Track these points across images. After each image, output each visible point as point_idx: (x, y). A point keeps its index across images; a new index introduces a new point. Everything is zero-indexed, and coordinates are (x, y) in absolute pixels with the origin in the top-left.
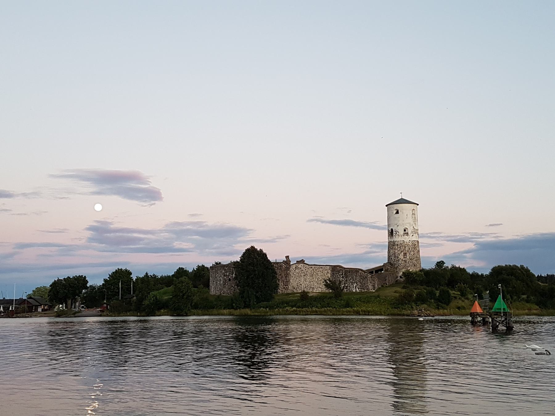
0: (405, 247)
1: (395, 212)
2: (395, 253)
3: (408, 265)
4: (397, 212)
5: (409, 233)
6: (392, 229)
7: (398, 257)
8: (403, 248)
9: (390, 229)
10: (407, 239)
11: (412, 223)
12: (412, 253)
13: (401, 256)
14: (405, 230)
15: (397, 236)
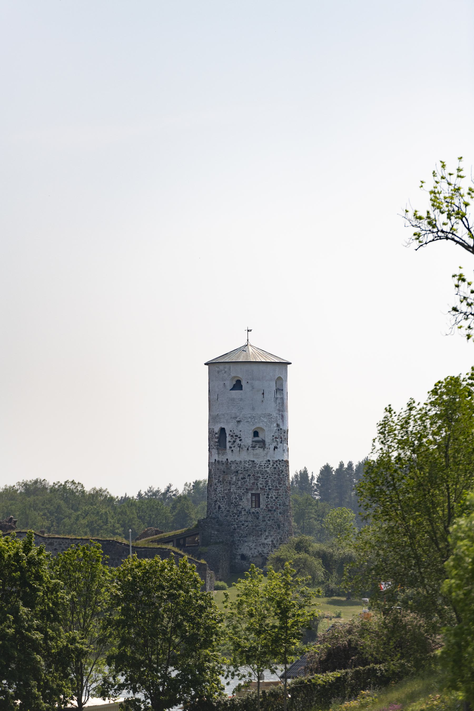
0: (257, 479)
1: (230, 384)
2: (229, 494)
3: (262, 525)
4: (238, 385)
5: (268, 440)
6: (223, 430)
7: (236, 506)
8: (250, 481)
9: (217, 430)
10: (260, 457)
11: (275, 414)
12: (273, 494)
13: (246, 503)
14: (256, 434)
15: (236, 449)
